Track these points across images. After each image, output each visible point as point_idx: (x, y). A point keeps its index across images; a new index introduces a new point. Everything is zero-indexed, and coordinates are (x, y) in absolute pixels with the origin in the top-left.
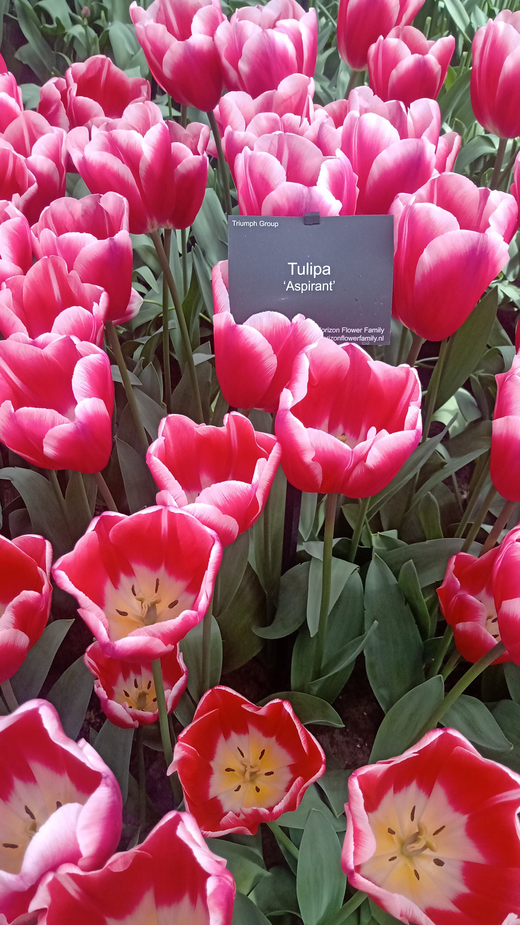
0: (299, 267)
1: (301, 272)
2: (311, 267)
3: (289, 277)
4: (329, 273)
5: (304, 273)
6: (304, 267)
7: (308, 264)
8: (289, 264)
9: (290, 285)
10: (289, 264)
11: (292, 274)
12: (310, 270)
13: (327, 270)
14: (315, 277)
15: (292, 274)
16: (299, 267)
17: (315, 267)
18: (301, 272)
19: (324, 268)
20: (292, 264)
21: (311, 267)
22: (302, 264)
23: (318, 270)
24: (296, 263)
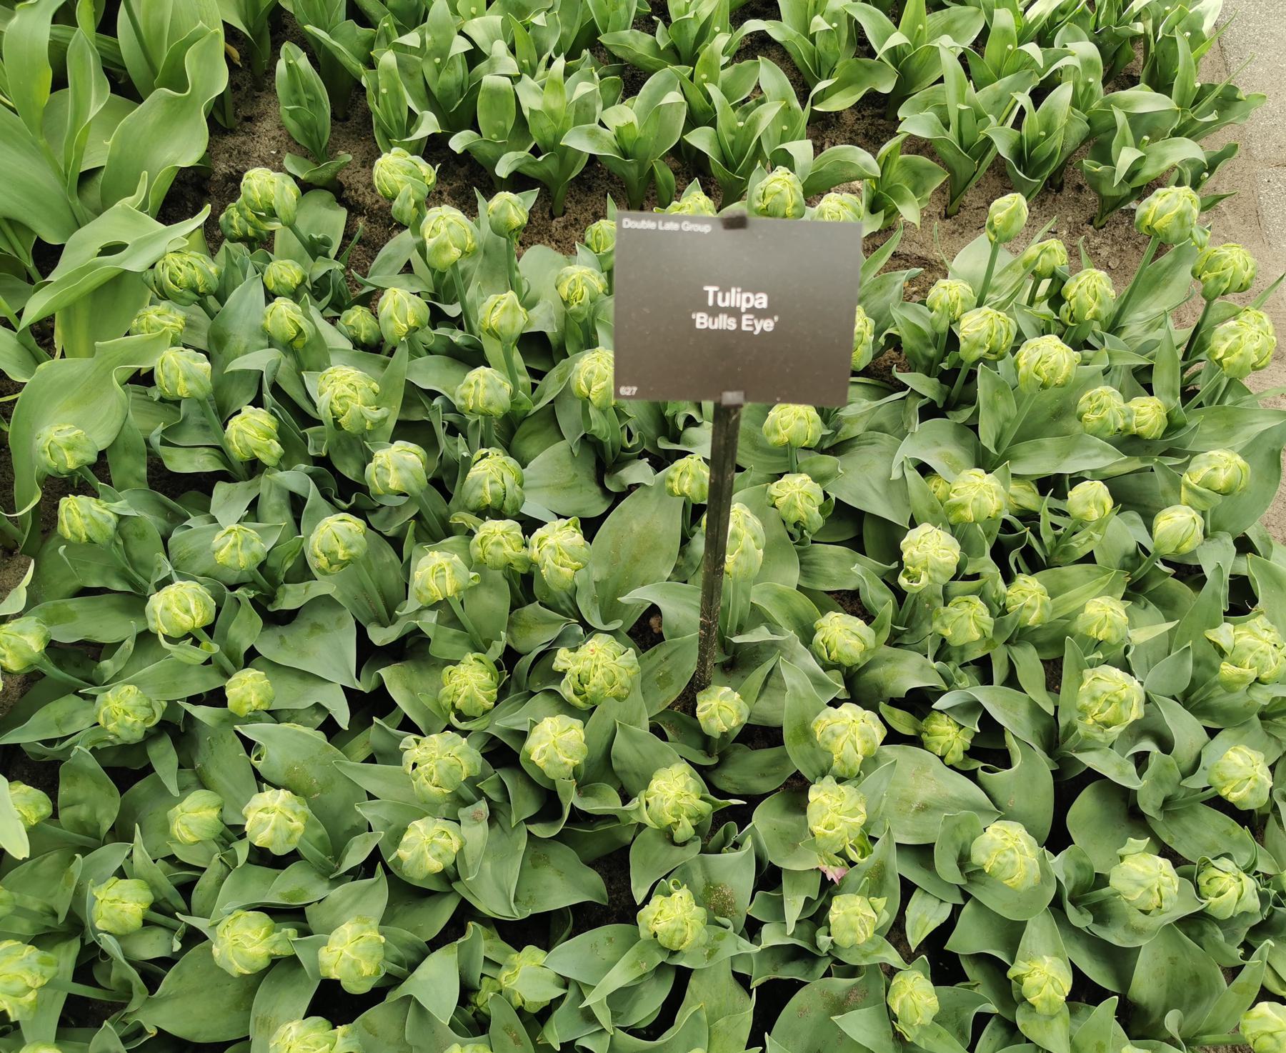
0: (720, 295)
1: (724, 300)
3: (703, 307)
4: (765, 305)
5: (727, 304)
6: (727, 295)
7: (733, 290)
8: (706, 288)
9: (702, 321)
11: (711, 303)
12: (736, 298)
13: (762, 301)
14: (743, 310)
15: (711, 303)
16: (720, 295)
17: (745, 296)
18: (724, 300)
20: (711, 289)
22: (725, 289)
23: (748, 300)
24: (716, 289)
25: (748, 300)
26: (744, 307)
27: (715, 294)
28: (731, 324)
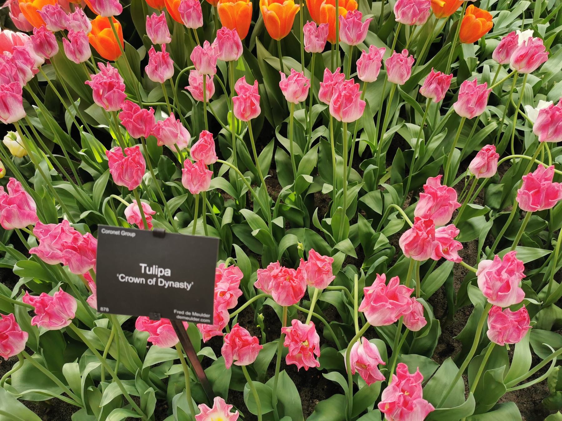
0: (147, 268)
1: (149, 271)
2: (157, 269)
5: (151, 273)
6: (151, 268)
7: (154, 266)
8: (141, 265)
10: (141, 265)
11: (143, 271)
15: (143, 271)
16: (147, 268)
17: (160, 269)
18: (149, 271)
19: (166, 270)
20: (143, 265)
21: (157, 269)
22: (150, 266)
23: (161, 272)
24: (146, 265)
25: (161, 272)
26: (159, 275)
27: (145, 268)
28: (152, 282)
